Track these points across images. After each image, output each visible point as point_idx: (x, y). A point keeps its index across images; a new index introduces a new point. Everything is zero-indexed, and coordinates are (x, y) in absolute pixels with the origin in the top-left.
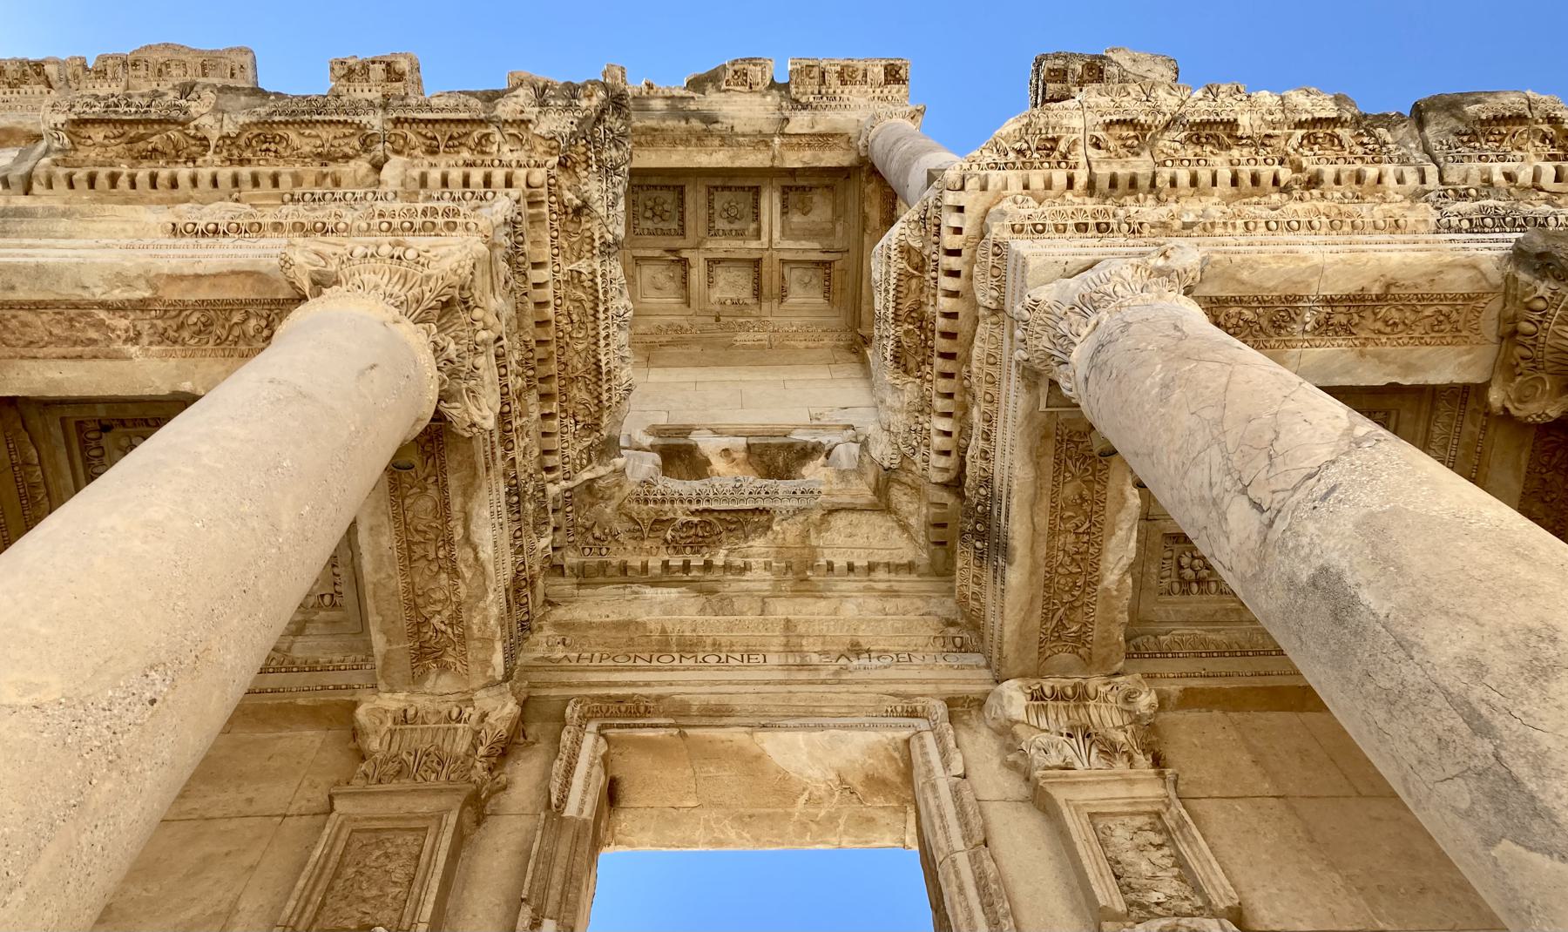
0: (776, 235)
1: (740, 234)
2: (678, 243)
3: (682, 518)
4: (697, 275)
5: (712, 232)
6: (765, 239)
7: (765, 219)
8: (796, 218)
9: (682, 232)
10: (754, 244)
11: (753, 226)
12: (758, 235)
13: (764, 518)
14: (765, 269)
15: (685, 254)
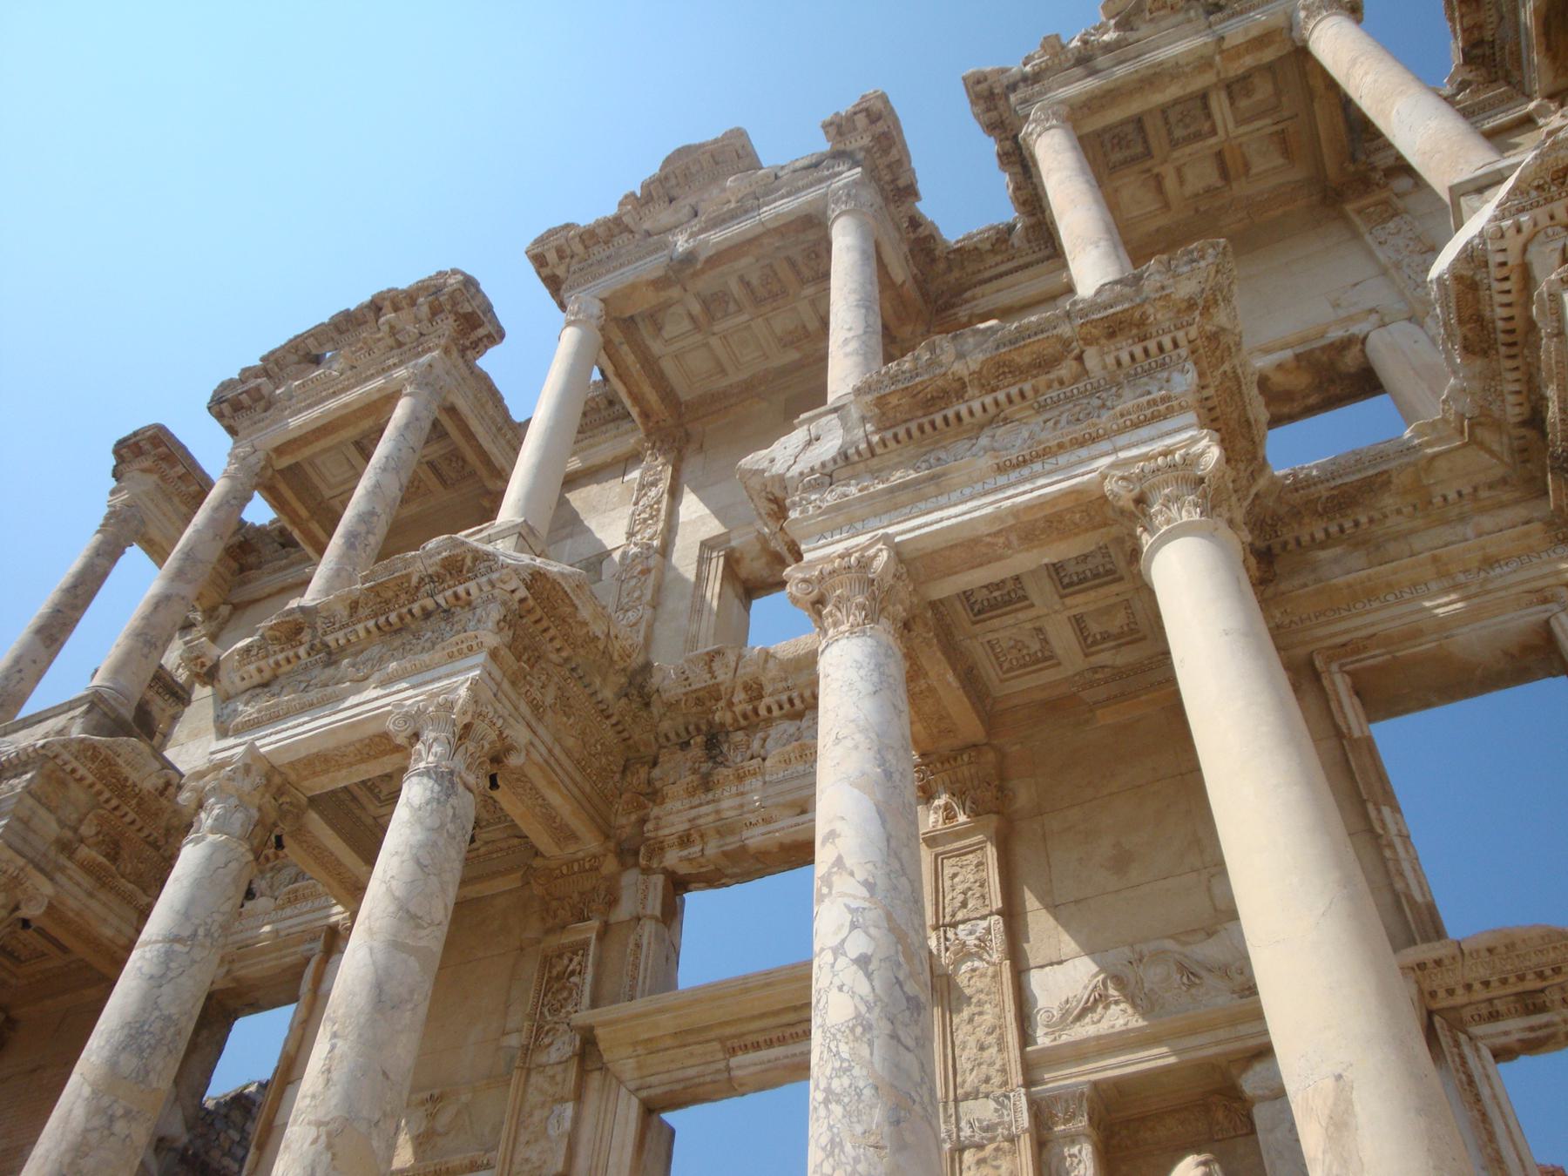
0: (1231, 125)
1: (1198, 136)
2: (1149, 164)
3: (1325, 494)
4: (1170, 183)
5: (1175, 144)
6: (1221, 132)
7: (1218, 117)
8: (1243, 103)
9: (1148, 154)
10: (1212, 141)
11: (1206, 126)
12: (1214, 132)
13: (1385, 477)
14: (1227, 155)
15: (1156, 170)
